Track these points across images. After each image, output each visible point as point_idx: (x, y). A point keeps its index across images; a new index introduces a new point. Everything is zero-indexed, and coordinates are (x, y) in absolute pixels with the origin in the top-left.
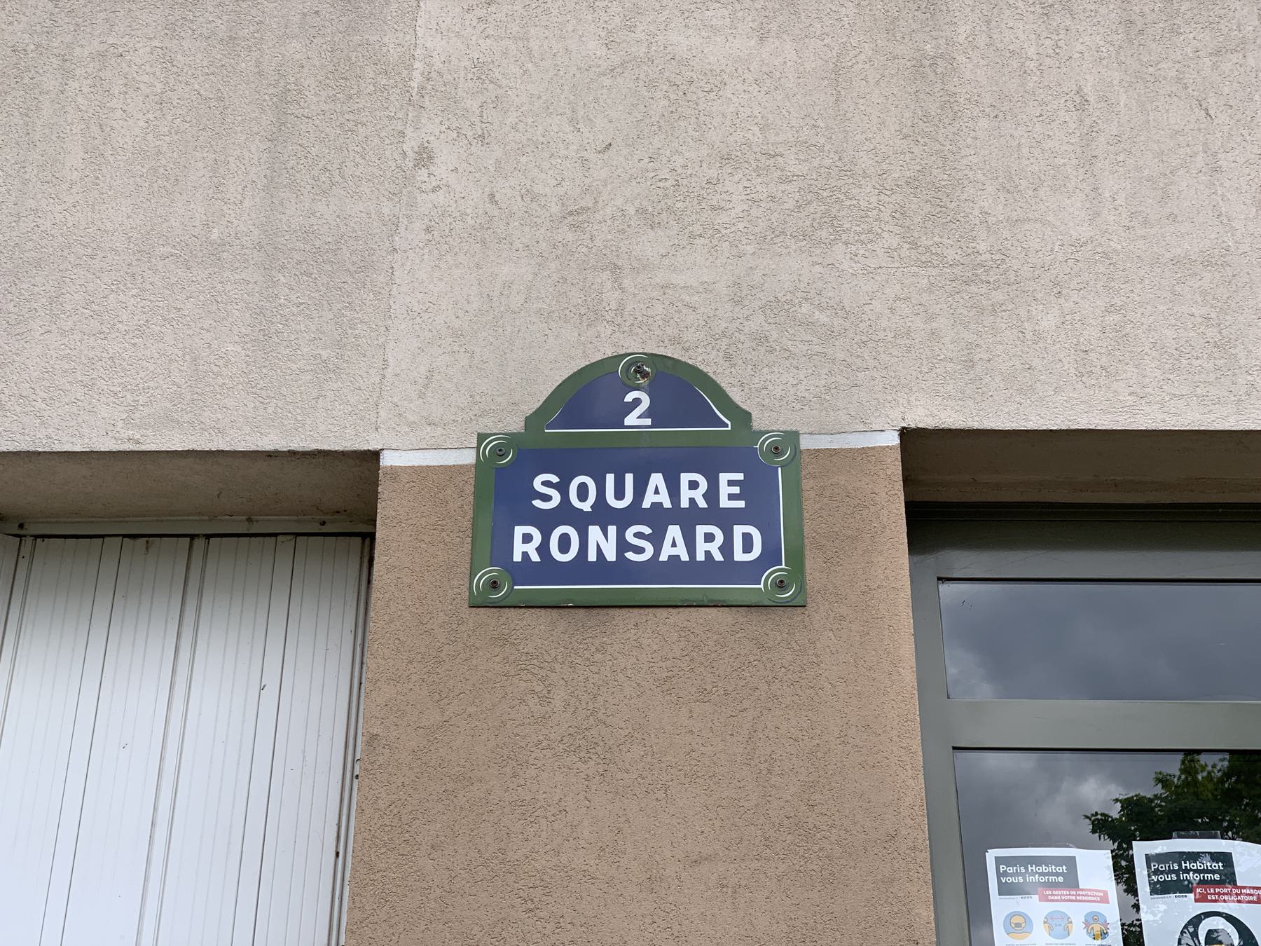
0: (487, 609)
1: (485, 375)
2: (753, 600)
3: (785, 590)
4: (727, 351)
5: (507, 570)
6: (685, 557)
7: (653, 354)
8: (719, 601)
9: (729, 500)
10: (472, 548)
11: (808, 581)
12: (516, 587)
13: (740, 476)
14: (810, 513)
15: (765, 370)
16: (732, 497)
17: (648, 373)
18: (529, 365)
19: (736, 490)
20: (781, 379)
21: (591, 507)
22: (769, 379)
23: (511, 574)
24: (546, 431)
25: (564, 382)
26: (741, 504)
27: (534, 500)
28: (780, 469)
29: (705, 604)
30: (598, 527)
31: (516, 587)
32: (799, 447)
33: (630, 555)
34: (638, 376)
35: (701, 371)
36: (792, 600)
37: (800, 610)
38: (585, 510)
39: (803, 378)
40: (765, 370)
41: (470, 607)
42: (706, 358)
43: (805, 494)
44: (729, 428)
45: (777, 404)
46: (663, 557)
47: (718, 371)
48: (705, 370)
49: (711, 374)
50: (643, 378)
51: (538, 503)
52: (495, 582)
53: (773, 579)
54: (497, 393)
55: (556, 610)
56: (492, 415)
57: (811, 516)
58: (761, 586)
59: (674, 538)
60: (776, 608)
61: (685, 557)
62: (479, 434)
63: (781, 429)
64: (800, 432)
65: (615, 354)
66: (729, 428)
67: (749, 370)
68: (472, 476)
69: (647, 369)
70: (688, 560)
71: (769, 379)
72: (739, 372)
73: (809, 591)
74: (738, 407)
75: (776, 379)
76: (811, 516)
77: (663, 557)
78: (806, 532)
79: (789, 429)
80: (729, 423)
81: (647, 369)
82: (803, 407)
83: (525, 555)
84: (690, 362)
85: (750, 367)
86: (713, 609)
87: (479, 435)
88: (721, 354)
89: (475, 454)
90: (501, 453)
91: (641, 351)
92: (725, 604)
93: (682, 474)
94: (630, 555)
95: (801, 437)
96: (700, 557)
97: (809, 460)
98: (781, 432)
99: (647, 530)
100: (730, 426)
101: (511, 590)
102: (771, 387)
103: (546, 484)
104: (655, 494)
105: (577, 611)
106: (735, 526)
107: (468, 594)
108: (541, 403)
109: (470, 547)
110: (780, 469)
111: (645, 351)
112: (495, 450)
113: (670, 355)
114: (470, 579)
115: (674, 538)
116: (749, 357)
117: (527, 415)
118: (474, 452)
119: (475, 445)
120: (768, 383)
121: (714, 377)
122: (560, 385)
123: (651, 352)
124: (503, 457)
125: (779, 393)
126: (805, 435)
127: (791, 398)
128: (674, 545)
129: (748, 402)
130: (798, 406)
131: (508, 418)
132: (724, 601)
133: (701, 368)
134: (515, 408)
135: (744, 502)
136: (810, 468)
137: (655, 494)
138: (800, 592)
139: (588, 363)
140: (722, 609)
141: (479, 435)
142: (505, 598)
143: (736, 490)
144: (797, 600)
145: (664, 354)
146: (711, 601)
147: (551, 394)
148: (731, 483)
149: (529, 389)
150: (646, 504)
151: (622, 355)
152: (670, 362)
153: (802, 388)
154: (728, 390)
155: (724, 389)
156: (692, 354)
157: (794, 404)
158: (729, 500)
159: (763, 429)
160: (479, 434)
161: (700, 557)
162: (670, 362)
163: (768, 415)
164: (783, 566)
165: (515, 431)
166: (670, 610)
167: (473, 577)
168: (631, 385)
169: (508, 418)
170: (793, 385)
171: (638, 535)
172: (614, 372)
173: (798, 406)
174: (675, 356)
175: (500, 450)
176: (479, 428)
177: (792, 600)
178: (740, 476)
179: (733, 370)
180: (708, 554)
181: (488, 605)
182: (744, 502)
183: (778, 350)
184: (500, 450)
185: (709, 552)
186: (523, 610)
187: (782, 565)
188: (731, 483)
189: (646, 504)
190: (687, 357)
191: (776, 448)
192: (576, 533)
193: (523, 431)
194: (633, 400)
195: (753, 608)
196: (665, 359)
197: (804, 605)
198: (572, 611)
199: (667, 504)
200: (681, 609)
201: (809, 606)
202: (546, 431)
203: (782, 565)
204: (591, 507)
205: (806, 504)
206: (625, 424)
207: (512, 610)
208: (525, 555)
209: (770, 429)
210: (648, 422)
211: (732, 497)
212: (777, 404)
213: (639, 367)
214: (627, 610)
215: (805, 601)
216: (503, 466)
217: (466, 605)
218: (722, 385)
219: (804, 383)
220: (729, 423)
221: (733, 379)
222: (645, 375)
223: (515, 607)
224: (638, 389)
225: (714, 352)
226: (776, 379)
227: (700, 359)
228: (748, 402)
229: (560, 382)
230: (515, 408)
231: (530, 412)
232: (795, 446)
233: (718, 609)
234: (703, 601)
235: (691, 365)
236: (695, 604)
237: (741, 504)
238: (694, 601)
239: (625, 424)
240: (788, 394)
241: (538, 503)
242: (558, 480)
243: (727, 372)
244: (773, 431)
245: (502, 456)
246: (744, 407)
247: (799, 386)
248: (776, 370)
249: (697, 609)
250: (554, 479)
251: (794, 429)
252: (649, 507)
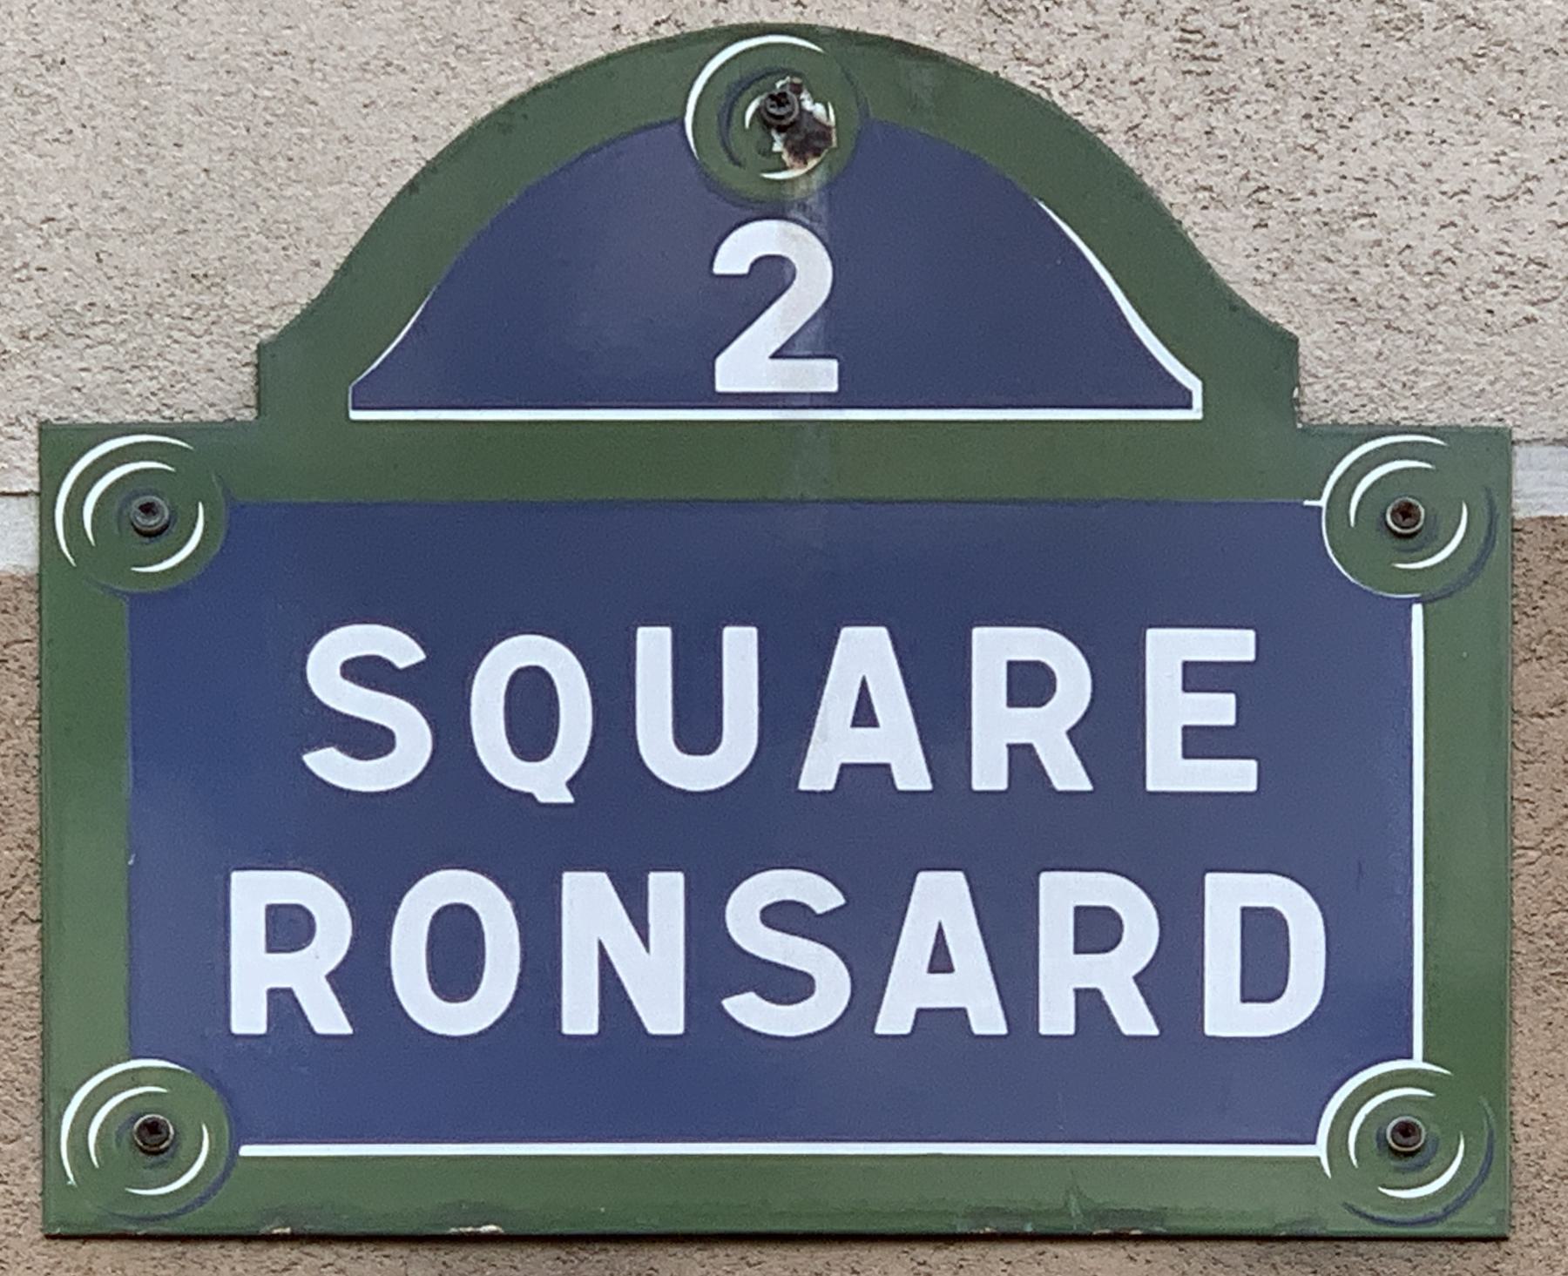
0: (125, 1246)
1: (55, 132)
2: (1286, 1213)
3: (1420, 1167)
4: (1194, 22)
5: (209, 1076)
6: (988, 1019)
7: (844, 34)
8: (1139, 1215)
9: (1187, 755)
10: (44, 968)
11: (1520, 1131)
12: (246, 1151)
13: (1237, 645)
14: (1547, 818)
15: (1369, 124)
16: (1199, 742)
17: (823, 133)
18: (258, 83)
19: (1220, 709)
20: (1437, 172)
21: (571, 784)
22: (1382, 168)
23: (219, 1086)
24: (355, 415)
25: (431, 170)
26: (1239, 776)
27: (312, 747)
28: (1417, 610)
29: (1075, 1227)
30: (603, 877)
31: (246, 1151)
32: (1509, 509)
33: (747, 1009)
34: (778, 147)
35: (1069, 127)
36: (1447, 1212)
37: (1479, 1255)
38: (542, 799)
39: (1539, 165)
40: (1369, 124)
41: (49, 1237)
42: (1093, 57)
43: (1526, 732)
44: (1195, 413)
45: (1418, 296)
46: (894, 1019)
47: (1149, 126)
48: (1088, 120)
49: (1116, 142)
50: (800, 151)
51: (329, 764)
52: (153, 1128)
53: (1368, 1117)
54: (119, 222)
55: (425, 1253)
56: (98, 332)
57: (1547, 831)
58: (1319, 1150)
59: (940, 932)
60: (1384, 1246)
61: (988, 1019)
62: (44, 429)
63: (1432, 420)
64: (1517, 435)
65: (666, 31)
66: (1195, 413)
67: (1292, 121)
68: (25, 632)
69: (819, 109)
70: (1002, 1030)
71: (1382, 168)
72: (1245, 128)
73: (1523, 1177)
74: (1236, 307)
75: (1419, 172)
76: (1547, 831)
77: (894, 1019)
78: (1524, 899)
79: (1464, 419)
80: (1193, 384)
81: (819, 109)
82: (1531, 311)
83: (283, 1003)
84: (1020, 77)
85: (1297, 106)
86: (1107, 1248)
87: (45, 430)
88: (1165, 40)
89: (34, 525)
90: (153, 522)
91: (789, 16)
92: (1158, 1229)
93: (978, 633)
94: (747, 1009)
95: (1521, 455)
96: (1057, 1018)
97: (1550, 568)
98: (1432, 431)
99: (822, 895)
100: (1197, 401)
101: (227, 1164)
102: (1389, 212)
103: (365, 671)
104: (855, 724)
105: (518, 1255)
106: (1210, 878)
107: (35, 1179)
108: (326, 275)
109: (35, 969)
110: (1417, 610)
111: (809, 18)
112: (129, 500)
113: (922, 40)
114: (44, 1112)
115: (940, 932)
116: (1293, 53)
117: (265, 335)
118: (25, 516)
119: (32, 484)
120: (1378, 188)
121: (1130, 157)
122: (412, 186)
123: (836, 22)
124: (163, 538)
125: (1429, 240)
126: (1536, 450)
127: (1482, 267)
128: (941, 961)
129: (1285, 281)
130: (1514, 308)
131: (176, 353)
132: (1159, 1214)
133: (1072, 105)
134: (206, 300)
135: (1251, 766)
136: (1551, 606)
137: (855, 724)
138: (1484, 1174)
139: (539, 77)
140: (1145, 1250)
141: (45, 430)
142: (202, 1201)
143: (1220, 709)
144: (1462, 1215)
145: (898, 35)
146: (1102, 1215)
147: (373, 227)
148: (1198, 677)
149: (267, 206)
150: (817, 774)
151: (701, 37)
152: (926, 76)
153: (1532, 214)
154: (1193, 220)
155: (1176, 214)
156: (1029, 36)
157: (1493, 298)
158: (1187, 755)
159: (1346, 418)
160: (44, 429)
161: (1057, 1018)
162: (926, 76)
163: (1373, 348)
164: (1417, 1062)
165: (212, 415)
166: (923, 1252)
167: (54, 1100)
168: (738, 185)
169: (176, 353)
170: (1496, 202)
171: (783, 916)
172: (670, 122)
173: (1514, 308)
174: (947, 46)
175: (148, 509)
176: (45, 400)
177: (1447, 1212)
178: (1237, 645)
179: (1217, 118)
180: (1089, 1003)
181: (132, 1228)
182: (1251, 766)
183: (1430, 20)
184: (148, 509)
185: (1096, 993)
186: (282, 1254)
187: (1410, 1056)
188: (1198, 677)
189: (817, 774)
190: (1005, 52)
191: (1406, 512)
192: (506, 906)
193: (249, 415)
194: (753, 265)
195: (1280, 1247)
196: (903, 62)
197: (1496, 1232)
198: (497, 1254)
199: (912, 774)
200: (970, 1252)
201: (1520, 1237)
202: (355, 415)
203: (1410, 1056)
204: (571, 784)
205: (1528, 776)
206: (720, 387)
207: (236, 1250)
208: (283, 1003)
209: (1381, 416)
210: (823, 375)
211: (1199, 742)
212: (1418, 296)
213: (780, 99)
214: (736, 1251)
215: (1506, 1216)
216: (171, 584)
217: (32, 1230)
218: (1166, 197)
219: (1545, 191)
220: (1193, 384)
221: (1218, 166)
222: (807, 140)
223: (246, 1239)
224: (776, 212)
225: (1134, 26)
226: (1419, 172)
227: (1064, 62)
228: (1285, 281)
229: (413, 171)
230: (206, 300)
231: (280, 320)
232: (1491, 502)
233: (1131, 1248)
234: (1063, 1212)
235: (1022, 92)
236: (1029, 1229)
237: (1239, 776)
238: (1024, 1216)
239: (720, 387)
240: (1468, 245)
241: (329, 764)
242: (418, 655)
243: (1191, 129)
244: (1397, 429)
245: (161, 537)
246: (1262, 308)
247: (1521, 209)
248: (1418, 125)
249: (1040, 1247)
250: (403, 651)
251: (1489, 419)
252: (830, 786)
